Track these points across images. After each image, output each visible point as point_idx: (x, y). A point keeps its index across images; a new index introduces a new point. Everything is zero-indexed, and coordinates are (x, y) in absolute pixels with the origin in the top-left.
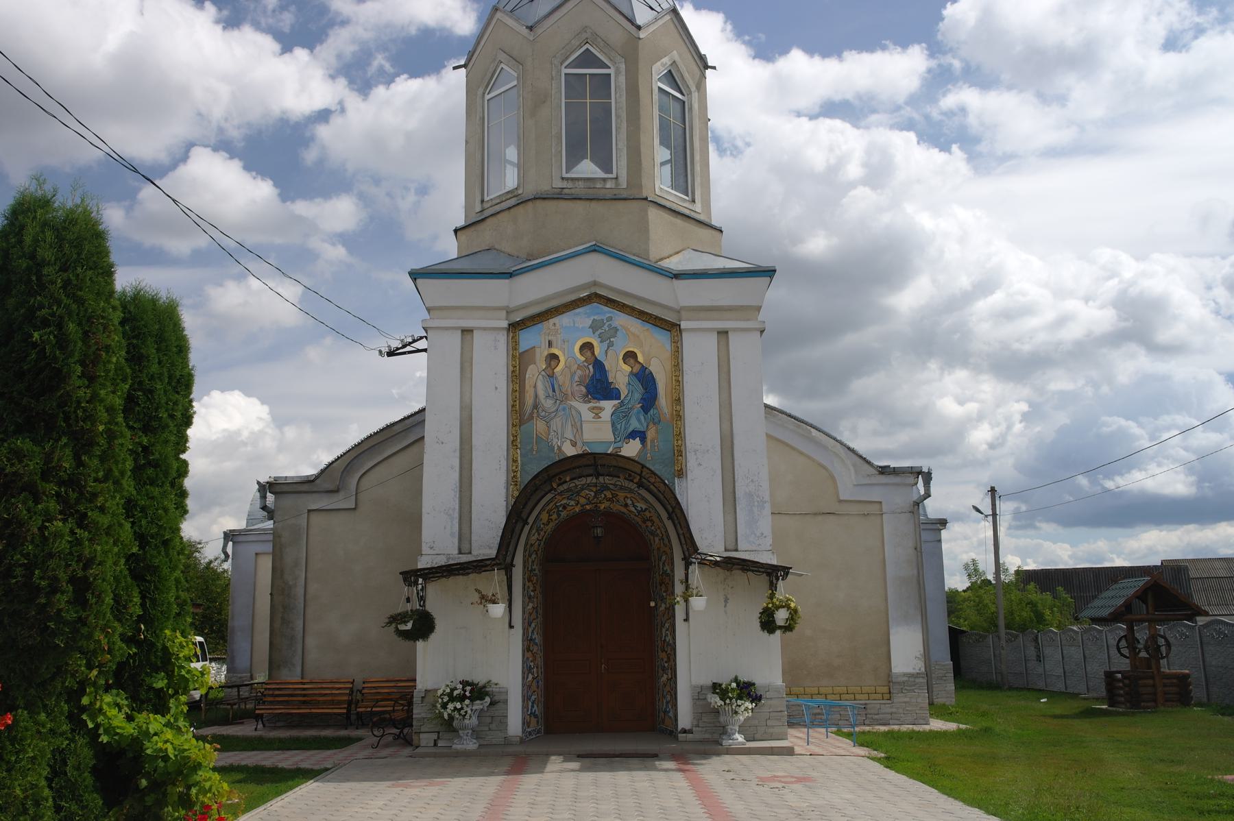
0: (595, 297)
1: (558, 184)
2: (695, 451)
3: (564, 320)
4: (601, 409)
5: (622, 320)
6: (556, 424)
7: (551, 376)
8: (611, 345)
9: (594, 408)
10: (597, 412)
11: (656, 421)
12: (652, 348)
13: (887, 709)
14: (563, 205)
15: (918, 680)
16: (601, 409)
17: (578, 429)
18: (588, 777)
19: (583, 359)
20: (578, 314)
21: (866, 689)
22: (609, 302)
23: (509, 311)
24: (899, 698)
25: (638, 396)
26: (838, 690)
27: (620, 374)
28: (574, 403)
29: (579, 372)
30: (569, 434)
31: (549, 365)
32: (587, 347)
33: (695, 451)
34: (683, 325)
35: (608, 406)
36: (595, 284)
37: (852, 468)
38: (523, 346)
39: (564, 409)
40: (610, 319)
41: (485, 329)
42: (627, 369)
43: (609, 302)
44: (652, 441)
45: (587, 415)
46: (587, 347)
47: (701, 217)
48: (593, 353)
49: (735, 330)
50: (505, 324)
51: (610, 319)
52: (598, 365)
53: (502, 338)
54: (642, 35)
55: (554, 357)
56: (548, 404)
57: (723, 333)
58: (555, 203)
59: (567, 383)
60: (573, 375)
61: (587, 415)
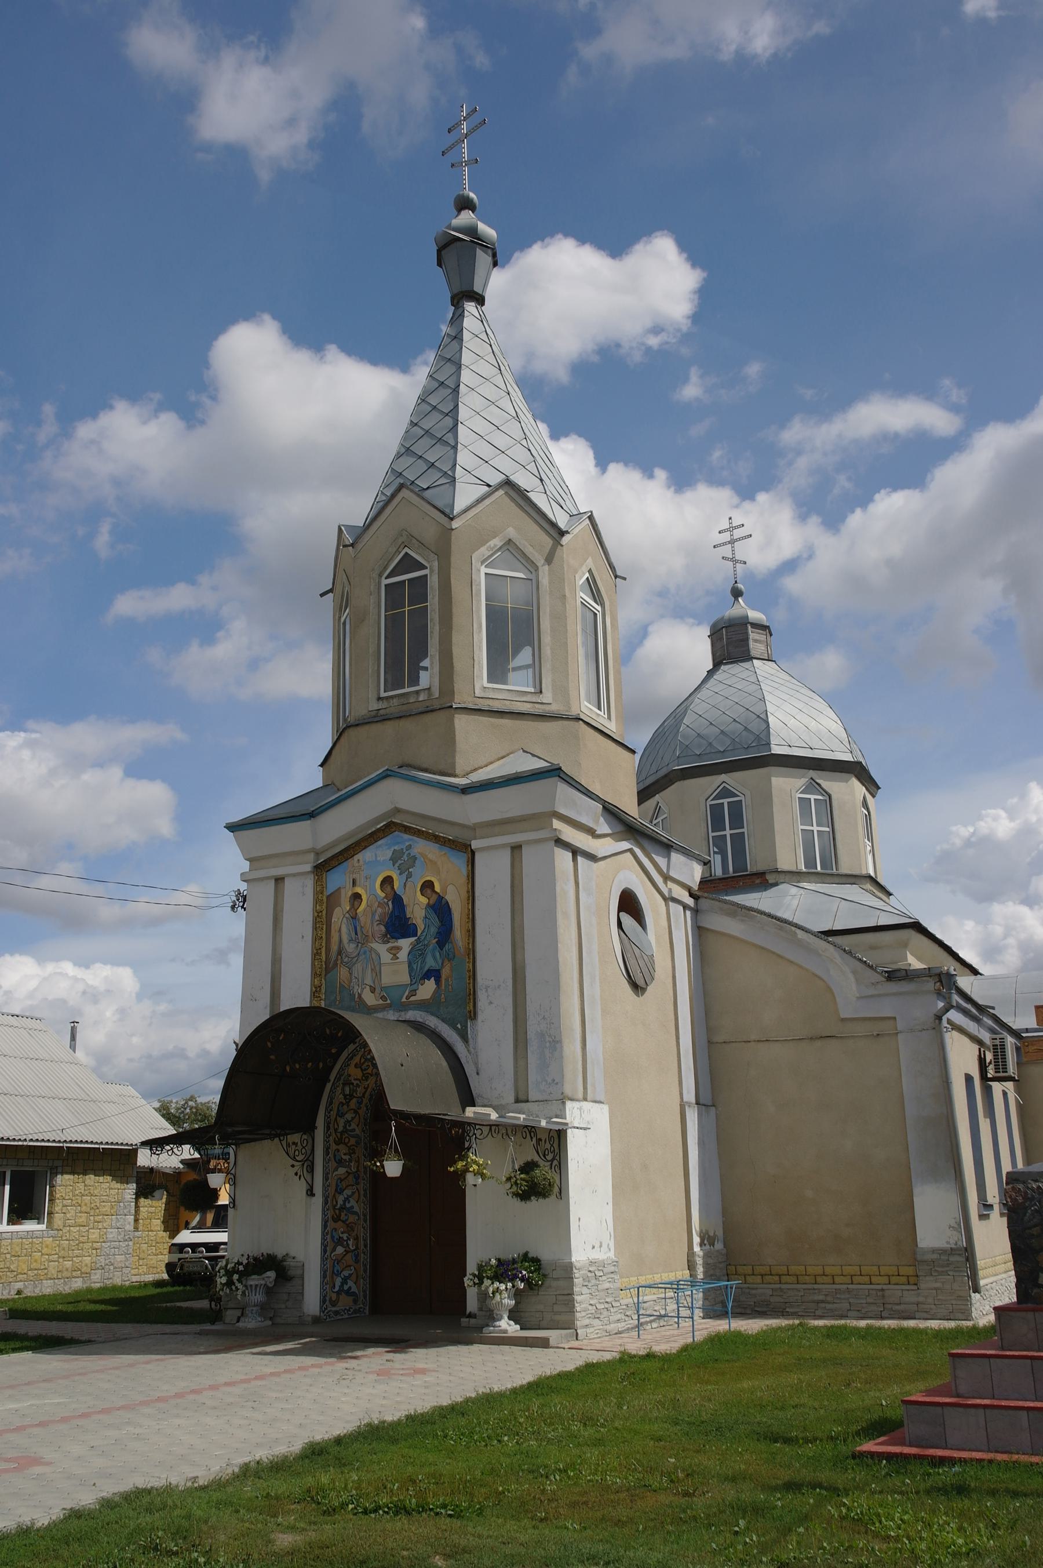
0: (389, 827)
1: (374, 706)
2: (487, 988)
3: (367, 855)
4: (399, 949)
5: (421, 847)
6: (358, 968)
7: (354, 917)
8: (410, 875)
9: (392, 948)
10: (395, 951)
11: (450, 957)
12: (444, 872)
13: (911, 1297)
14: (375, 728)
15: (952, 1259)
16: (399, 949)
17: (377, 973)
18: (398, 1357)
19: (383, 895)
20: (380, 846)
21: (884, 1270)
22: (407, 829)
23: (317, 854)
24: (928, 1283)
25: (433, 930)
26: (848, 1270)
27: (417, 907)
28: (375, 945)
29: (380, 910)
30: (368, 981)
31: (352, 906)
32: (388, 881)
33: (487, 988)
34: (475, 845)
35: (405, 944)
36: (397, 811)
37: (851, 976)
38: (331, 888)
39: (365, 953)
40: (409, 847)
41: (294, 875)
42: (424, 900)
43: (407, 829)
44: (447, 980)
45: (386, 957)
46: (388, 881)
47: (555, 708)
48: (393, 888)
49: (529, 842)
50: (308, 868)
51: (409, 847)
52: (397, 900)
53: (310, 882)
54: (455, 524)
55: (357, 897)
56: (350, 948)
57: (516, 849)
58: (367, 727)
59: (369, 922)
60: (373, 915)
61: (386, 957)
